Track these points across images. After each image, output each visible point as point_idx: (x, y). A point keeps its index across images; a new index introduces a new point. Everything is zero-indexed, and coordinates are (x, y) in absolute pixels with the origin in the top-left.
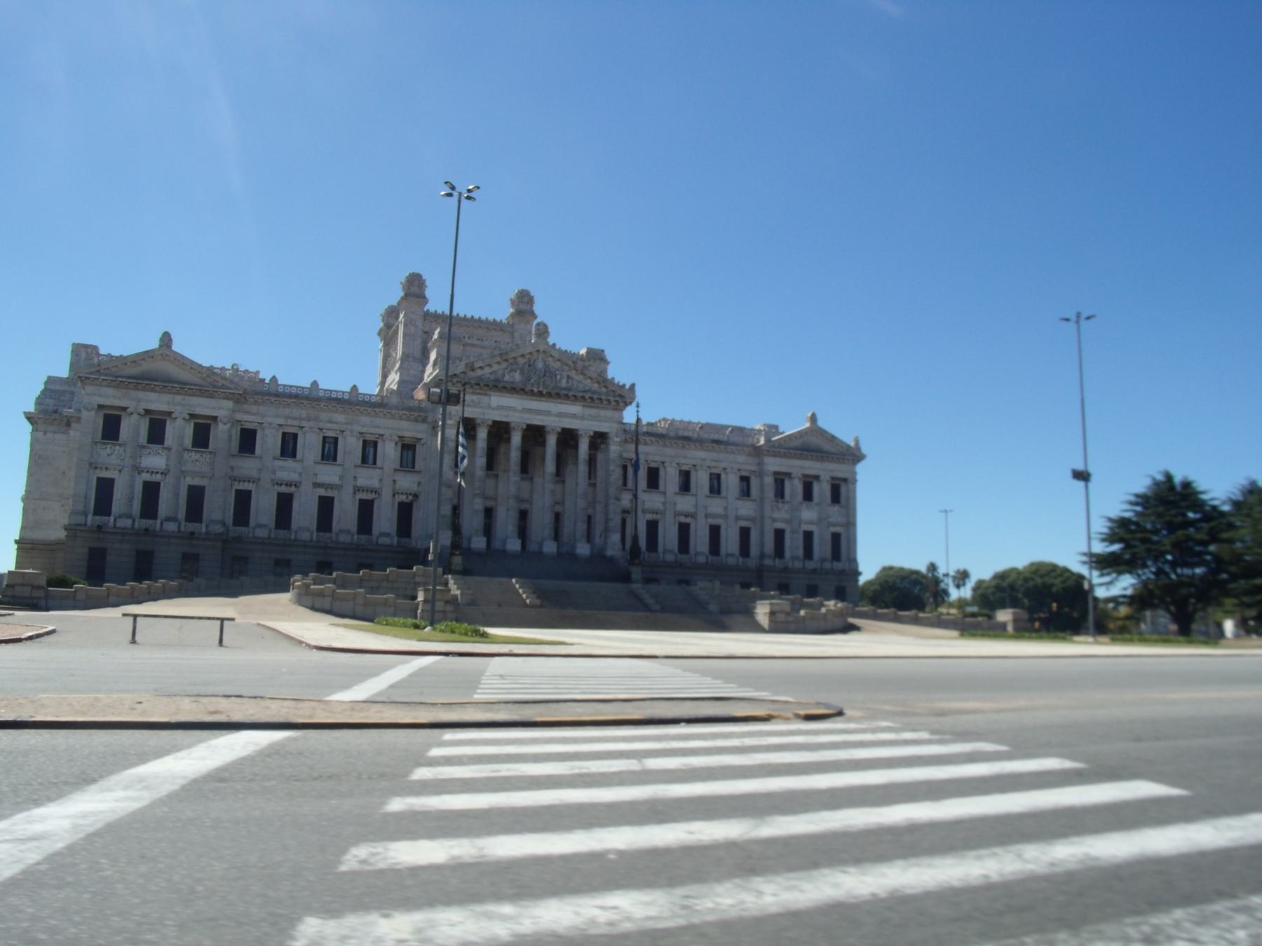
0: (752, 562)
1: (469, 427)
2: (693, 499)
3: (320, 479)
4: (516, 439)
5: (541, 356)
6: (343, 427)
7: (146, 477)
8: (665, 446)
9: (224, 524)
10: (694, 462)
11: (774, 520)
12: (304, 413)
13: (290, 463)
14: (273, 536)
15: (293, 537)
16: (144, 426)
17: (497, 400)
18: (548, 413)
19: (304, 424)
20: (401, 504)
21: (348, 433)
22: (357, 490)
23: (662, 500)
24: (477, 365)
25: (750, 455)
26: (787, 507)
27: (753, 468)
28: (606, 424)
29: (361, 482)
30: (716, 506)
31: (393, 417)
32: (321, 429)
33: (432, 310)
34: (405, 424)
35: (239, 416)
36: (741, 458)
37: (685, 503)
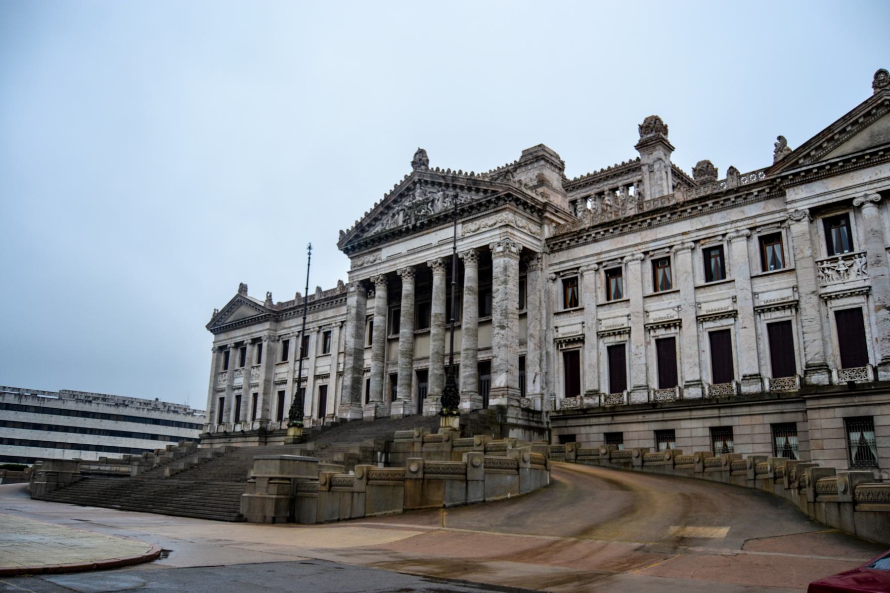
0: (792, 385)
1: (367, 287)
4: (407, 287)
7: (237, 392)
8: (622, 234)
9: (265, 420)
10: (670, 242)
11: (826, 299)
16: (238, 353)
17: (386, 252)
18: (428, 247)
23: (626, 311)
24: (365, 224)
26: (858, 263)
27: (778, 217)
28: (488, 235)
30: (716, 299)
32: (320, 327)
36: (752, 210)
37: (662, 309)
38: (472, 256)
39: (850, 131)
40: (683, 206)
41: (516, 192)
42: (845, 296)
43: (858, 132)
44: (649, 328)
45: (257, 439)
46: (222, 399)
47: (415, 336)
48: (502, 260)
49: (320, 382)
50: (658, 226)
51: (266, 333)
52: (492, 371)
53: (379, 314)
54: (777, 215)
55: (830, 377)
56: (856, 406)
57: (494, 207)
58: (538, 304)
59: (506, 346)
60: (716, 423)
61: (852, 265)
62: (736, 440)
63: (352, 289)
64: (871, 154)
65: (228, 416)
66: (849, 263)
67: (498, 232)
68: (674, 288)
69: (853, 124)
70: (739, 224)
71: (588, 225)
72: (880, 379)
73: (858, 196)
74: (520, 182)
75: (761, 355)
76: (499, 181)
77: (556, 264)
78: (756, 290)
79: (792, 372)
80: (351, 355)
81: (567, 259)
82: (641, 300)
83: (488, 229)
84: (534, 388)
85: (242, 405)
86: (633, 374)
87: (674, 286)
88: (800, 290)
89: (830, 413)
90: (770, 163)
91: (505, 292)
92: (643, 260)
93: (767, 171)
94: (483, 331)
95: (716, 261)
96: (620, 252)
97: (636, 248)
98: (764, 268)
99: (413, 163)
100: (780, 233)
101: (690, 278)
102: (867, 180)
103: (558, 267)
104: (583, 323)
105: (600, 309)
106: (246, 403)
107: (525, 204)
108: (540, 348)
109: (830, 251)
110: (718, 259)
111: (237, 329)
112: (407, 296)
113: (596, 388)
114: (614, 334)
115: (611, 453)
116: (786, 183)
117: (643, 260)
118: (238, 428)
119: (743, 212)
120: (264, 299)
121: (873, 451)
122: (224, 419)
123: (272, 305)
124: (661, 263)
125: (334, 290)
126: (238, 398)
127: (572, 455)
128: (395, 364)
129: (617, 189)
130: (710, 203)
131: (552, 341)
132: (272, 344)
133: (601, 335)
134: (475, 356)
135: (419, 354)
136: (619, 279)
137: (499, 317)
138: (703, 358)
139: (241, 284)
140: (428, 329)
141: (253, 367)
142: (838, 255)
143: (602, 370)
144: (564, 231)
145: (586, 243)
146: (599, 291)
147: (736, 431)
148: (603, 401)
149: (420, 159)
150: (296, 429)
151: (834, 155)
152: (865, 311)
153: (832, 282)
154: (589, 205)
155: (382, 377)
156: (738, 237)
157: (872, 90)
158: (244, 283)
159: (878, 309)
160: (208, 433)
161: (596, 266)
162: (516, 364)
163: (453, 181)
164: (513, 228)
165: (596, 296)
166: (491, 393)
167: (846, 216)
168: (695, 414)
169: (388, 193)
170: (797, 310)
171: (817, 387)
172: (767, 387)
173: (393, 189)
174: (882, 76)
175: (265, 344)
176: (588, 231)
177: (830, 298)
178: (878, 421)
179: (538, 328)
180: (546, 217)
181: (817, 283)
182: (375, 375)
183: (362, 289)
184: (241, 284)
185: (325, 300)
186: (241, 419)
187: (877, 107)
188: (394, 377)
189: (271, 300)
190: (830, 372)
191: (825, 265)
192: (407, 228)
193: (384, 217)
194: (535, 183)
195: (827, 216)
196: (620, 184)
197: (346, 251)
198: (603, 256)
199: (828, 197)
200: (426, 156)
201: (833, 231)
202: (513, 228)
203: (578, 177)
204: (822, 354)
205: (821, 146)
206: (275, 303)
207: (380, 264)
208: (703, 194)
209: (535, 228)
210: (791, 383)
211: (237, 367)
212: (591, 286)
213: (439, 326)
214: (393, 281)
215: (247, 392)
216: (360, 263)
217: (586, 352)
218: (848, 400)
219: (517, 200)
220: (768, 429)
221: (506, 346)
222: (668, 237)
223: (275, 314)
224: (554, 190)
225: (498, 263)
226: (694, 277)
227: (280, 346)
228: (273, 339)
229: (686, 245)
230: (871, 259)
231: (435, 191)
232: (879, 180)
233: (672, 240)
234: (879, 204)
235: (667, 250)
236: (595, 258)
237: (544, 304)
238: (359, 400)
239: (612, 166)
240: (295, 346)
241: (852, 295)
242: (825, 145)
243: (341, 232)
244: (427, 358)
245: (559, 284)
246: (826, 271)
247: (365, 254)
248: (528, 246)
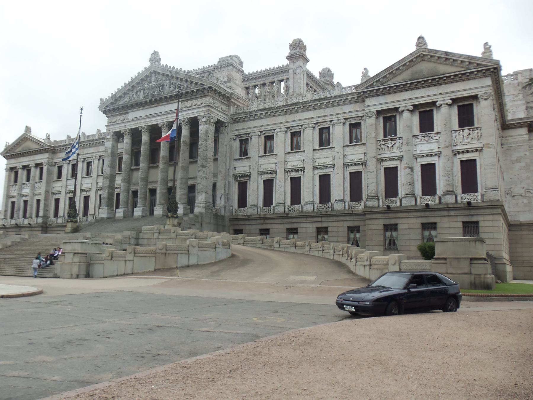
0: (359, 207)
1: (119, 136)
4: (145, 138)
7: (25, 198)
8: (275, 116)
9: (46, 217)
16: (25, 173)
17: (132, 115)
18: (159, 115)
21: (94, 158)
25: (356, 102)
26: (398, 142)
27: (360, 114)
28: (197, 110)
30: (324, 157)
32: (84, 159)
35: (55, 161)
36: (348, 108)
37: (295, 160)
38: (187, 122)
39: (402, 69)
40: (310, 102)
41: (215, 86)
42: (390, 160)
43: (406, 70)
44: (287, 171)
45: (40, 229)
46: (13, 203)
47: (149, 168)
48: (205, 126)
49: (84, 194)
50: (295, 113)
51: (46, 160)
52: (196, 192)
53: (126, 153)
54: (360, 113)
55: (379, 203)
56: (390, 218)
58: (225, 153)
59: (206, 178)
60: (319, 225)
61: (395, 144)
62: (330, 234)
63: (109, 137)
64: (411, 84)
65: (18, 214)
66: (394, 142)
67: (203, 109)
68: (302, 149)
69: (403, 66)
70: (340, 116)
71: (256, 109)
72: (403, 205)
73: (402, 106)
74: (217, 79)
75: (345, 189)
76: (205, 78)
77: (237, 130)
78: (345, 154)
79: (360, 199)
80: (107, 178)
81: (242, 128)
82: (284, 155)
84: (220, 202)
85: (28, 206)
86: (277, 196)
87: (302, 148)
88: (368, 156)
89: (377, 222)
90: (359, 82)
91: (206, 144)
92: (286, 132)
93: (357, 87)
94: (192, 167)
95: (326, 135)
96: (274, 126)
97: (283, 125)
98: (351, 142)
99: (151, 60)
100: (360, 123)
101: (311, 144)
102: (407, 98)
103: (237, 132)
104: (250, 166)
105: (260, 158)
106: (32, 206)
107: (220, 93)
108: (225, 179)
109: (385, 136)
110: (327, 134)
111: (24, 156)
112: (145, 144)
113: (256, 203)
114: (268, 173)
115: (263, 240)
116: (366, 95)
117: (286, 132)
118: (26, 222)
119: (342, 109)
120: (45, 138)
121: (396, 242)
122: (15, 216)
123: (50, 142)
124: (296, 135)
125: (94, 135)
126: (26, 202)
127: (242, 241)
128: (137, 184)
129: (274, 82)
130: (325, 102)
131: (232, 175)
132: (50, 167)
133: (260, 174)
134: (187, 183)
135: (151, 179)
136: (272, 142)
137: (202, 160)
138: (315, 189)
139: (27, 127)
140: (157, 164)
141: (36, 182)
142: (389, 138)
143: (259, 193)
144: (242, 111)
145: (254, 119)
146: (260, 148)
147: (329, 229)
148: (259, 211)
149: (155, 58)
150: (73, 223)
151: (392, 83)
152: (399, 169)
153: (384, 152)
154: (257, 91)
155: (128, 193)
156: (339, 123)
157: (416, 47)
158: (29, 126)
159: (405, 168)
160: (4, 225)
161: (259, 133)
162: (211, 187)
163: (176, 75)
164: (212, 107)
165: (259, 151)
166: (196, 205)
167: (395, 116)
168: (309, 220)
169: (134, 78)
170: (365, 166)
171: (372, 207)
172: (347, 207)
173: (137, 75)
174: (421, 40)
175: (45, 168)
176: (256, 112)
177: (382, 160)
178: (400, 227)
179: (224, 168)
180: (232, 102)
181: (377, 152)
182: (123, 191)
183: (116, 137)
184: (27, 127)
185: (88, 141)
186: (28, 215)
187: (416, 57)
188: (135, 193)
189: (49, 139)
190: (378, 200)
191: (382, 143)
192: (146, 102)
193: (131, 92)
194: (226, 79)
195: (385, 115)
196: (276, 79)
197: (105, 112)
198: (263, 128)
199: (387, 105)
200: (159, 56)
201: (388, 124)
202: (212, 107)
203: (251, 72)
204: (376, 190)
205: (386, 76)
206: (52, 140)
207: (127, 122)
208: (321, 97)
209: (225, 108)
210: (359, 205)
211: (24, 182)
212: (256, 145)
213: (165, 163)
214: (136, 134)
215: (32, 199)
216: (114, 120)
217: (251, 183)
218: (386, 215)
219: (216, 90)
220: (346, 229)
221: (206, 178)
222: (301, 120)
223: (52, 149)
224: (237, 85)
225: (202, 128)
226: (313, 144)
227: (56, 170)
228: (51, 164)
229: (310, 125)
230: (404, 141)
231: (164, 79)
232: (413, 99)
233: (303, 121)
234: (412, 111)
235: (300, 127)
236: (259, 128)
237: (228, 153)
238: (113, 206)
239: (272, 68)
240: (66, 170)
241: (393, 159)
242: (388, 76)
243: (101, 99)
244: (156, 182)
245: (238, 142)
246: (382, 146)
247: (118, 115)
248: (220, 119)
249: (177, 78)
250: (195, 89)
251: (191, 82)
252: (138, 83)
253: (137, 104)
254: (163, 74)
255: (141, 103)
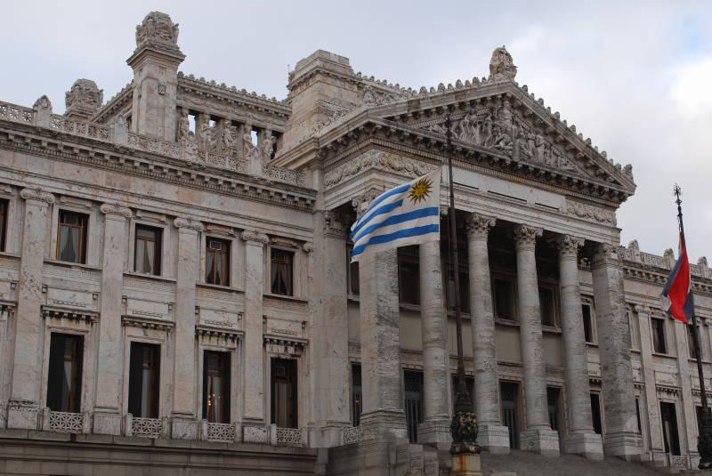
2: (673, 362)
3: (134, 308)
5: (507, 103)
6: (172, 210)
12: (101, 177)
13: (74, 276)
14: (46, 426)
15: (86, 428)
18: (520, 203)
19: (101, 196)
20: (276, 362)
22: (200, 333)
28: (598, 230)
29: (207, 317)
31: (257, 199)
32: (134, 210)
33: (186, 74)
34: (277, 214)
44: (659, 390)
57: (607, 200)
67: (609, 233)
83: (594, 221)
163: (566, 134)
192: (502, 161)
216: (397, 164)
249: (565, 142)
250: (586, 182)
251: (595, 167)
252: (473, 103)
253: (477, 154)
254: (533, 117)
255: (489, 158)
